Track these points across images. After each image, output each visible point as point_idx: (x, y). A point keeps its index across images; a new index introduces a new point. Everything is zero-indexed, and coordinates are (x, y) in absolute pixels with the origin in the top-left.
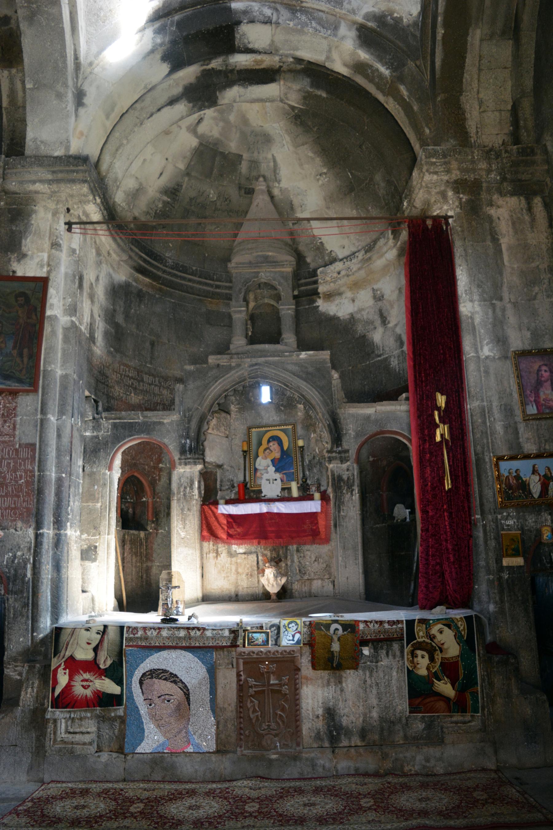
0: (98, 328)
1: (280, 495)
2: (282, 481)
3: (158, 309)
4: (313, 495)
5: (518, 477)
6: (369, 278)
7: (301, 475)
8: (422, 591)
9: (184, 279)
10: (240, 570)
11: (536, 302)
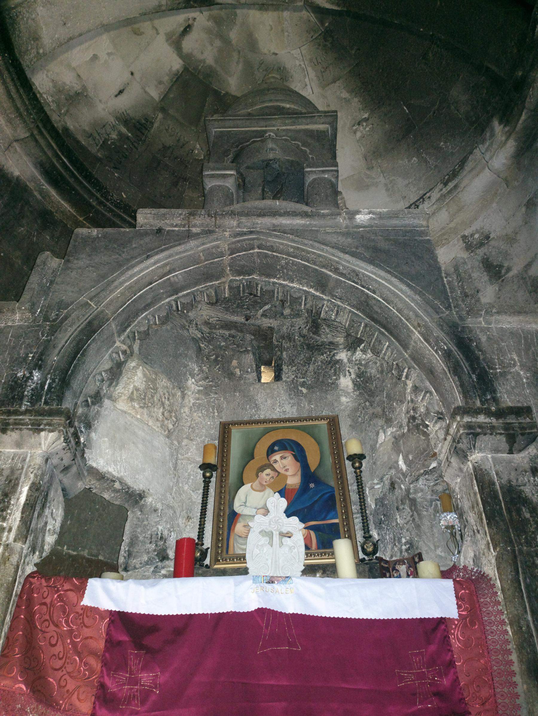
2: (307, 547)
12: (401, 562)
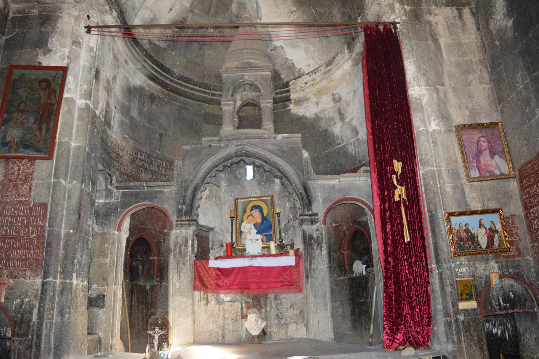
0: (114, 117)
1: (261, 252)
2: (262, 241)
3: (166, 109)
4: (288, 252)
5: (467, 231)
6: (329, 86)
7: (278, 237)
8: (386, 333)
9: (188, 87)
10: (226, 316)
11: (471, 87)
12: (288, 245)
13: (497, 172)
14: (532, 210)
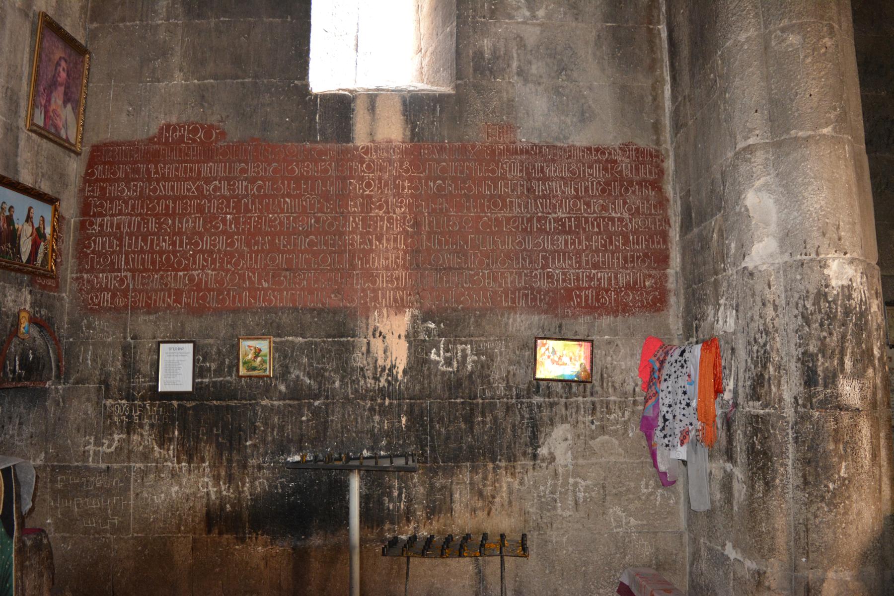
5: (10, 220)
13: (63, 134)
14: (99, 220)
